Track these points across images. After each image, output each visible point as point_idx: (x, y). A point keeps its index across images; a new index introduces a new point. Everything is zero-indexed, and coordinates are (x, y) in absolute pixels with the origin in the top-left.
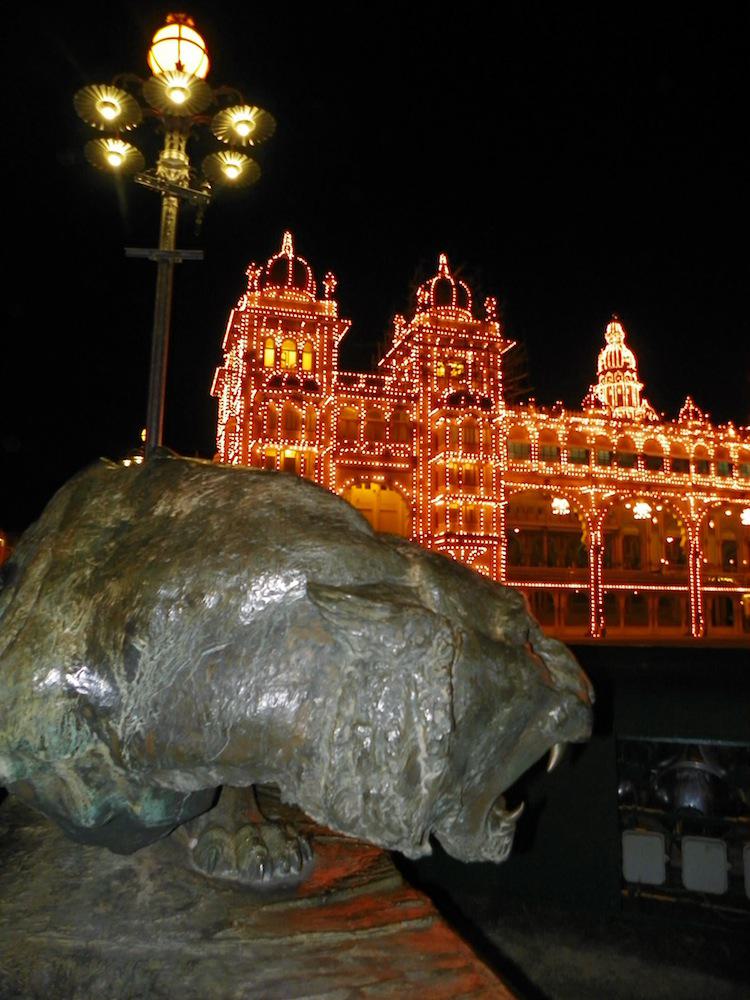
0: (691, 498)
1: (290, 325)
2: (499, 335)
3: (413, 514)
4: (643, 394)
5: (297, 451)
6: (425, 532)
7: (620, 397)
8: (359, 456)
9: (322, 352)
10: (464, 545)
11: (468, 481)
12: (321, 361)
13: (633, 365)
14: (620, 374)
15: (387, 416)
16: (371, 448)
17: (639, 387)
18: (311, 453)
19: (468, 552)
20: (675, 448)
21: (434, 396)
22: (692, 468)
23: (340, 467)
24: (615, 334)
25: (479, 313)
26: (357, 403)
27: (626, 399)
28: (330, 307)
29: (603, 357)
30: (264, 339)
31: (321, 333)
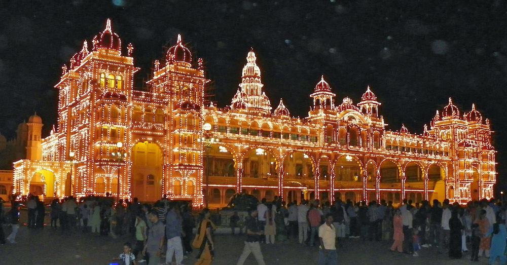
0: (281, 149)
1: (113, 69)
2: (203, 76)
3: (164, 155)
4: (263, 89)
5: (117, 127)
7: (252, 91)
8: (142, 129)
9: (126, 81)
10: (187, 169)
11: (188, 142)
12: (126, 86)
13: (259, 75)
14: (253, 79)
15: (154, 111)
17: (262, 85)
18: (123, 128)
19: (188, 172)
20: (275, 127)
21: (175, 103)
22: (282, 136)
23: (133, 134)
24: (251, 57)
25: (195, 66)
26: (140, 105)
27: (255, 92)
28: (130, 60)
29: (245, 69)
30: (100, 74)
31: (127, 72)
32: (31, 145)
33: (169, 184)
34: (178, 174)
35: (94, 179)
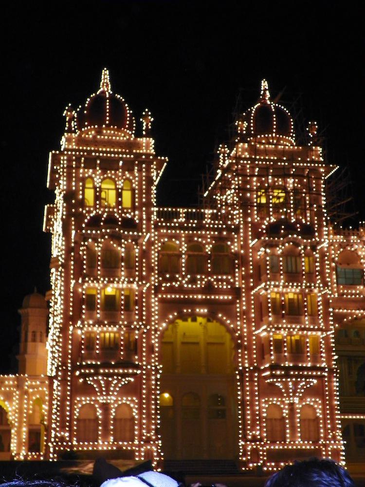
1: (108, 165)
2: (321, 159)
3: (239, 346)
5: (117, 289)
6: (251, 364)
8: (181, 290)
9: (141, 189)
10: (291, 377)
11: (292, 311)
12: (141, 198)
15: (208, 249)
16: (193, 281)
18: (131, 290)
19: (296, 384)
21: (255, 226)
23: (162, 301)
26: (177, 237)
28: (148, 145)
30: (83, 180)
31: (140, 171)
32: (25, 352)
33: (253, 414)
34: (271, 390)
35: (72, 411)
